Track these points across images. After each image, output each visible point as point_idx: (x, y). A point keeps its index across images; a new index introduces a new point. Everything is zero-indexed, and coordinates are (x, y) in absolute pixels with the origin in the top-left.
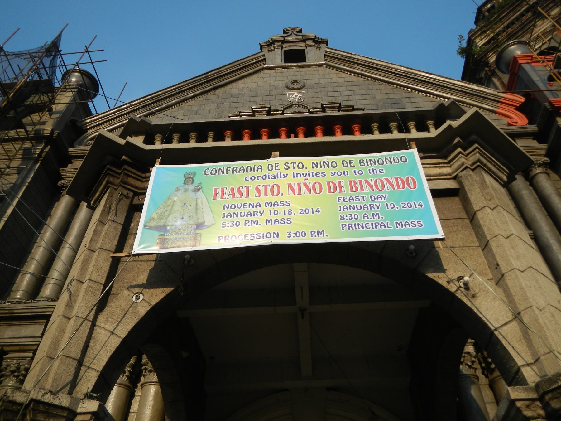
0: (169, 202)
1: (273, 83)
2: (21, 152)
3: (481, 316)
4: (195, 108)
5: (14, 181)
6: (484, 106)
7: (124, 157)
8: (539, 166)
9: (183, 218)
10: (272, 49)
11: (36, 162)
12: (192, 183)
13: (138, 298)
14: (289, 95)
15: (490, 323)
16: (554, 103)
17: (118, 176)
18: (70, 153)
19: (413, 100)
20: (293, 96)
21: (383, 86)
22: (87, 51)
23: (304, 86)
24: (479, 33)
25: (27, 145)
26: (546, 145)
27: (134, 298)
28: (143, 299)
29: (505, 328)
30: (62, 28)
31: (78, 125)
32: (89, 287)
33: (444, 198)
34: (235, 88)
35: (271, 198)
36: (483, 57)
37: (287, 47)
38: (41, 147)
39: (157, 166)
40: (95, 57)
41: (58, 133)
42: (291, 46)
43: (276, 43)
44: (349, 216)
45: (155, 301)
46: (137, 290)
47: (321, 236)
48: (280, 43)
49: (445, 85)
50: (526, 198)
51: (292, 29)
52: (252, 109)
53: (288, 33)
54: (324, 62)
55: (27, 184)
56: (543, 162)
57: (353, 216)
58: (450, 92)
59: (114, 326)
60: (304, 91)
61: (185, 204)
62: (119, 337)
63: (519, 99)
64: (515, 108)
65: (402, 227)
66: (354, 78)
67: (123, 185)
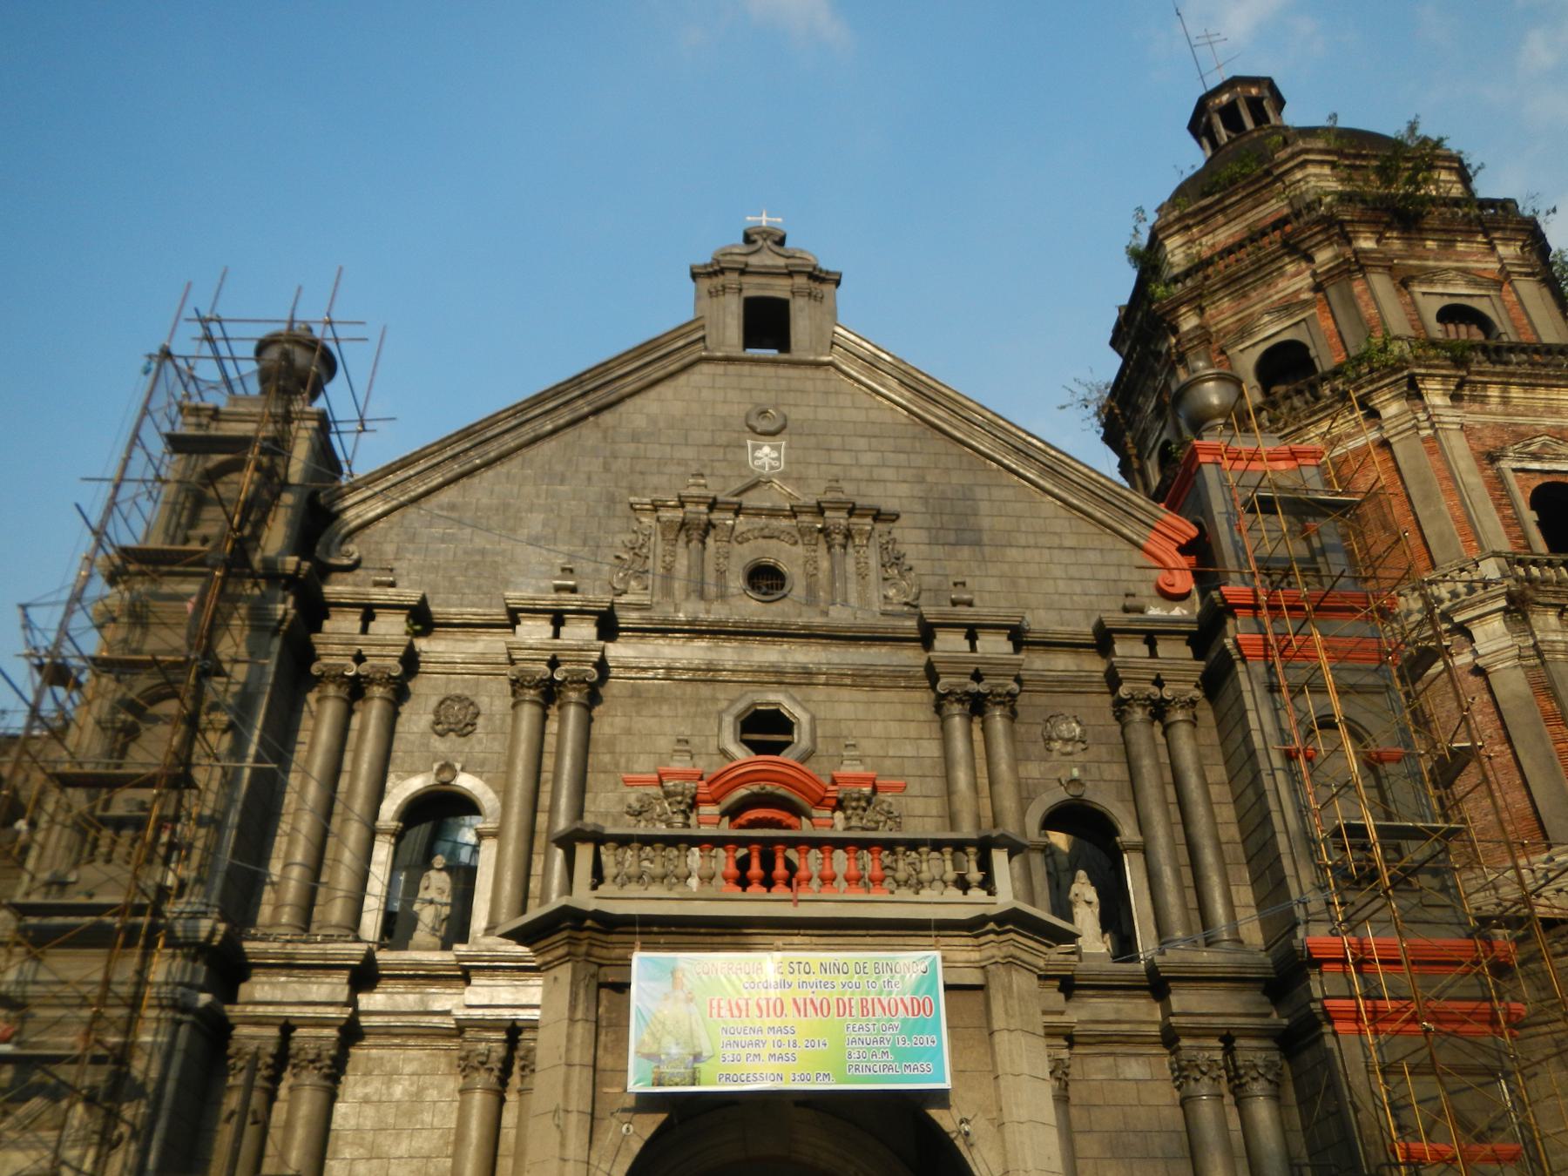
1: (722, 410)
6: (1125, 531)
8: (1182, 707)
19: (997, 493)
21: (941, 444)
23: (784, 427)
24: (1176, 228)
26: (1203, 663)
30: (291, 305)
36: (1167, 313)
37: (755, 288)
40: (342, 332)
42: (760, 287)
45: (647, 1134)
49: (1060, 469)
50: (1146, 776)
52: (679, 497)
53: (754, 242)
55: (268, 689)
56: (1191, 699)
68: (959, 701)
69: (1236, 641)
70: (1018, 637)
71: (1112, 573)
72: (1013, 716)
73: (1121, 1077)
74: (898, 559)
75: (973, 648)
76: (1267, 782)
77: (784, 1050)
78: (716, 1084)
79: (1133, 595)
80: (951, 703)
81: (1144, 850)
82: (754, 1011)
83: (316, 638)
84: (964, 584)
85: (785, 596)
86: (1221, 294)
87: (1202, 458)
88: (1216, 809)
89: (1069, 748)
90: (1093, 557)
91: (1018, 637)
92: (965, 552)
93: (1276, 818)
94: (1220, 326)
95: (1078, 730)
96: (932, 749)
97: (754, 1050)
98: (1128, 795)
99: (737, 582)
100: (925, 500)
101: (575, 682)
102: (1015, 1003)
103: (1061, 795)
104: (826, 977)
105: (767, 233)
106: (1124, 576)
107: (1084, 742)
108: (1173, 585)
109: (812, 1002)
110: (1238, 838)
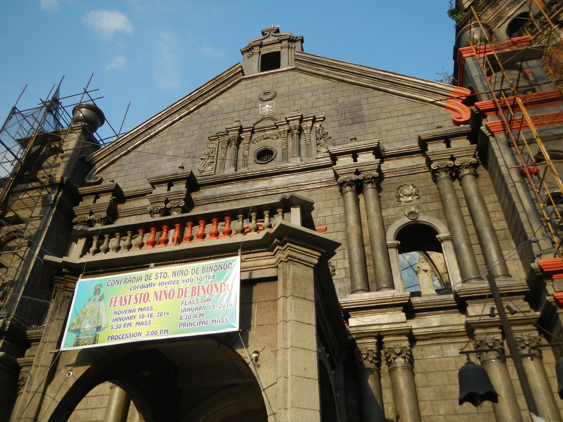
0: (84, 309)
1: (249, 96)
2: (40, 200)
3: (258, 380)
4: (181, 131)
5: (38, 226)
7: (64, 270)
8: (466, 168)
9: (90, 323)
10: (251, 55)
11: (53, 208)
12: (99, 294)
13: (69, 374)
14: (262, 107)
15: (262, 385)
16: (479, 107)
17: (62, 282)
18: (80, 192)
19: (371, 100)
20: (264, 109)
21: (345, 87)
22: (86, 92)
23: (275, 96)
25: (45, 193)
26: (476, 145)
27: (67, 375)
28: (72, 375)
29: (269, 389)
31: (87, 160)
32: (40, 370)
33: (270, 282)
34: (214, 105)
35: (143, 305)
37: (265, 51)
38: (54, 195)
39: (80, 281)
40: (93, 95)
41: (67, 179)
43: (255, 48)
44: (185, 317)
45: (78, 376)
46: (69, 368)
47: (166, 333)
48: (258, 48)
51: (270, 30)
53: (266, 34)
54: (294, 67)
55: (47, 228)
56: (471, 163)
57: (188, 317)
58: (404, 89)
59: (55, 394)
60: (274, 101)
61: (92, 311)
62: (57, 402)
63: (465, 92)
64: (461, 101)
65: (215, 323)
66: (321, 81)
67: (65, 289)
68: (349, 185)
69: (486, 126)
70: (378, 152)
71: (431, 121)
72: (379, 189)
73: (445, 355)
74: (324, 135)
75: (355, 160)
76: (512, 190)
77: (146, 319)
78: (106, 342)
79: (441, 127)
80: (345, 187)
81: (451, 239)
82: (133, 300)
83: (75, 208)
84: (355, 139)
85: (273, 159)
86: (486, 8)
87: (464, 55)
88: (492, 215)
89: (410, 198)
90: (419, 116)
91: (378, 152)
92: (357, 126)
93: (518, 206)
94: (488, 22)
95: (414, 190)
96: (339, 210)
97: (127, 322)
98: (442, 215)
99: (252, 158)
100: (337, 110)
101: (175, 208)
102: (289, 282)
103: (406, 220)
104: (176, 278)
105: (270, 30)
106: (436, 120)
107: (417, 195)
108: (461, 118)
109: (165, 291)
110: (506, 226)
